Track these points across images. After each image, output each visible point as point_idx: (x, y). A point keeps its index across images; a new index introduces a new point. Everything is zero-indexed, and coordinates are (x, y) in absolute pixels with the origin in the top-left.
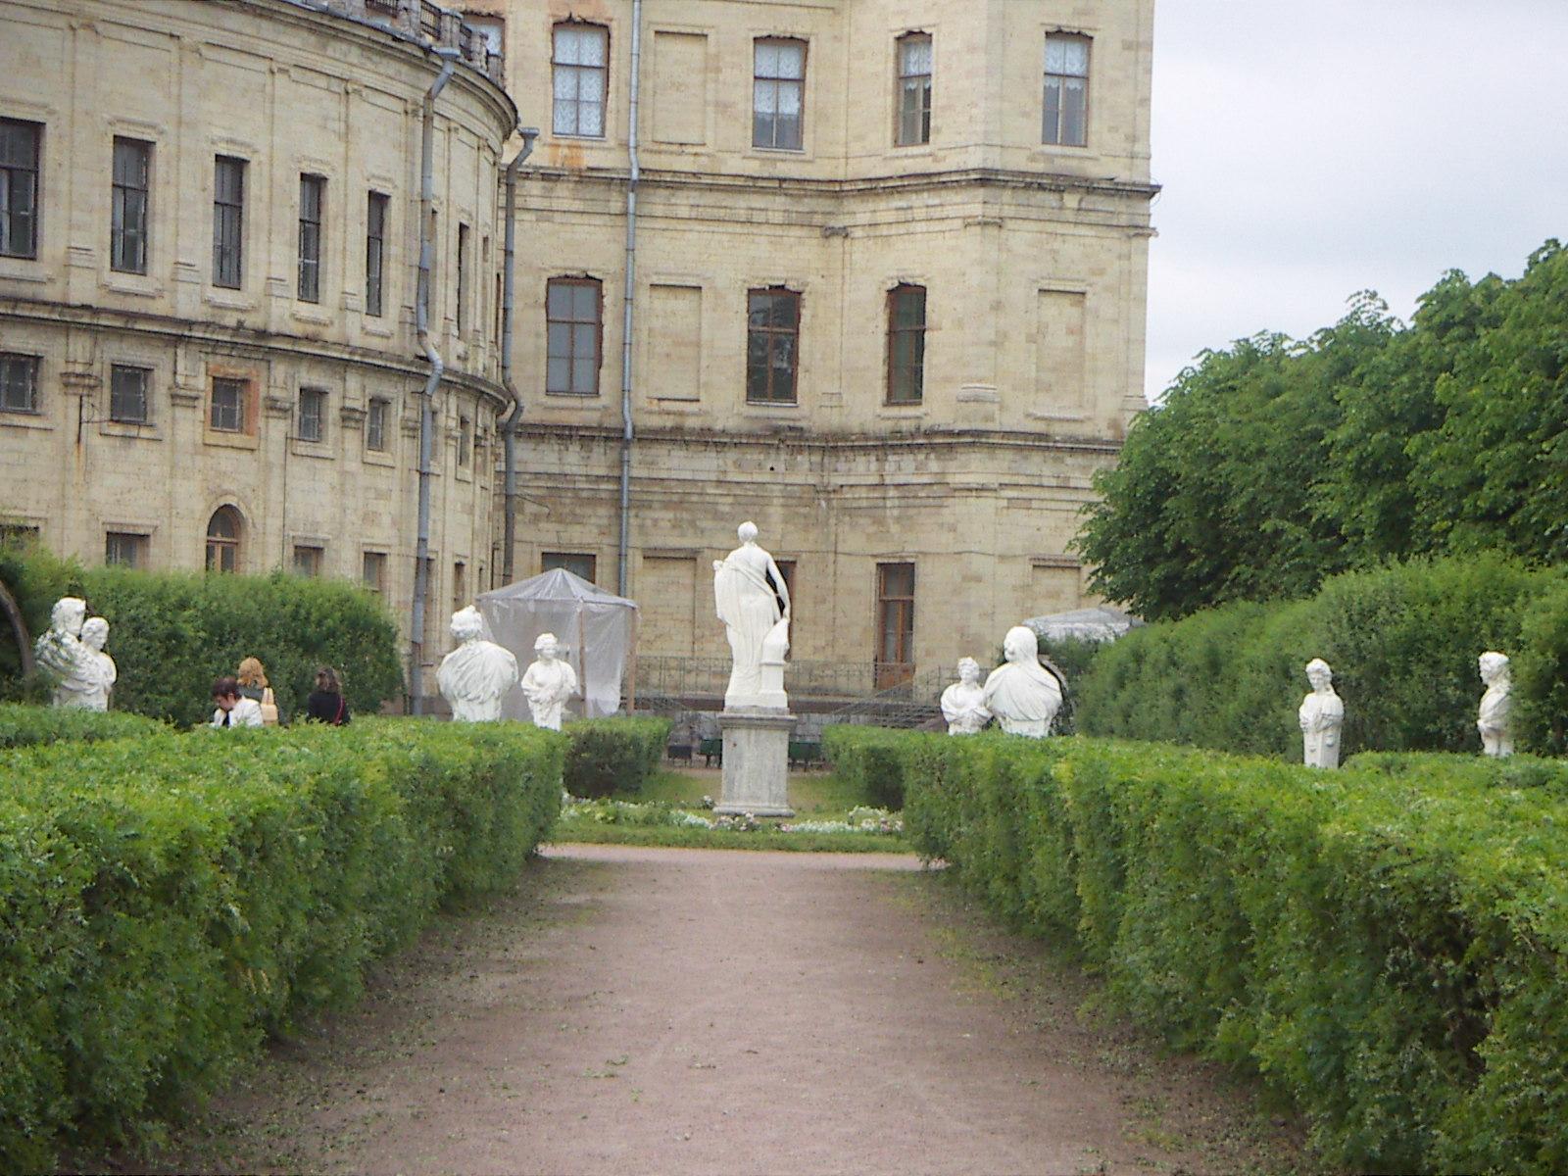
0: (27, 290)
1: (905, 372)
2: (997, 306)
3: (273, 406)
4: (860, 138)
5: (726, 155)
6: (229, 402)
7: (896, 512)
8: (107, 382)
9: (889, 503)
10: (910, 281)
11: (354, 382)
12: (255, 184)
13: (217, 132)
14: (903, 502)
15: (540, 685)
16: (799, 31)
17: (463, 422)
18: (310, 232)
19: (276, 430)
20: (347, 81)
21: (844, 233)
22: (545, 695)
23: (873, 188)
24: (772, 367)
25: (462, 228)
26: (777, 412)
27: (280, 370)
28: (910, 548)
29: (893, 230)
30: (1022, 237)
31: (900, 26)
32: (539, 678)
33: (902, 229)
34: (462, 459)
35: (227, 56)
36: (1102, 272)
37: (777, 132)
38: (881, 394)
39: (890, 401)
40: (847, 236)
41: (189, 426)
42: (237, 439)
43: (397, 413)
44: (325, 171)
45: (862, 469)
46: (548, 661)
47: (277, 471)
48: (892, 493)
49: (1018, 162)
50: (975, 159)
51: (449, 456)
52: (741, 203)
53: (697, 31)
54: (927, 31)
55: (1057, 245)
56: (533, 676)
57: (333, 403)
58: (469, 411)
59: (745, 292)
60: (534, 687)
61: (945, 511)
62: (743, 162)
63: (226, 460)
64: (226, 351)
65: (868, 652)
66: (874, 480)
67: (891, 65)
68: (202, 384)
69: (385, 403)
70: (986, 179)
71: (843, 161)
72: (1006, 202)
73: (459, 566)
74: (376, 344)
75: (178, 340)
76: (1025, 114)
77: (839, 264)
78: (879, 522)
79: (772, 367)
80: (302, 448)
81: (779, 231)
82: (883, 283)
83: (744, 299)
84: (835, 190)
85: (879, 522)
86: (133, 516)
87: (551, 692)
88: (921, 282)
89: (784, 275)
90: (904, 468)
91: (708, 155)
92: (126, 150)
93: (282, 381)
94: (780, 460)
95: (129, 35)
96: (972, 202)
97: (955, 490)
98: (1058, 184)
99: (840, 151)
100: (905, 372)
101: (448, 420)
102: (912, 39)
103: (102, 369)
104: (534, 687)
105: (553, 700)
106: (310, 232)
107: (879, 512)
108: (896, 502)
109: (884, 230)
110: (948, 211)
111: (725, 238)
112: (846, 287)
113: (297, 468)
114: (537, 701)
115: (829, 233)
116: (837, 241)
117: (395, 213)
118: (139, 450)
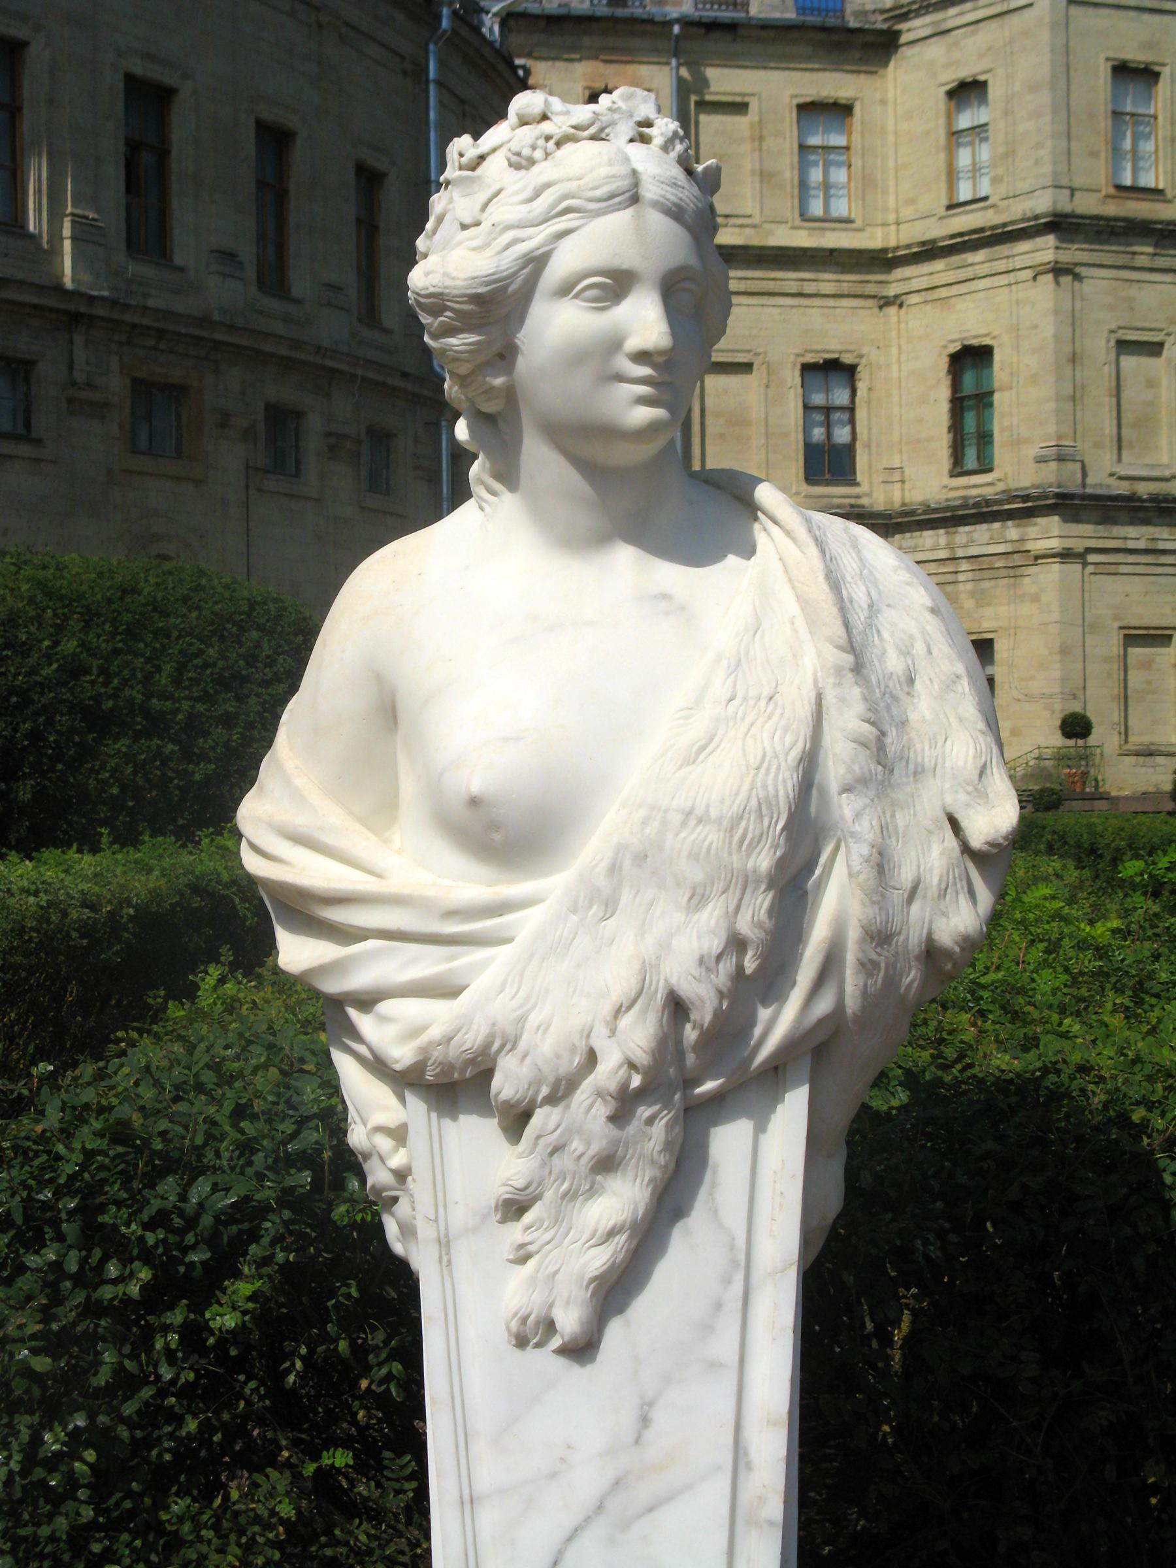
2: (1074, 359)
4: (912, 201)
5: (773, 226)
7: (969, 586)
9: (961, 577)
10: (975, 342)
14: (978, 575)
15: (503, 833)
18: (273, 193)
19: (229, 458)
20: (318, 9)
21: (896, 301)
22: (576, 973)
23: (929, 252)
28: (986, 625)
29: (954, 290)
30: (1098, 286)
32: (481, 733)
33: (964, 288)
39: (958, 468)
40: (901, 306)
44: (291, 121)
48: (964, 566)
49: (1087, 205)
50: (1042, 204)
52: (790, 279)
53: (738, 99)
54: (982, 78)
55: (1133, 291)
56: (388, 712)
57: (314, 423)
59: (799, 367)
60: (414, 866)
61: (1026, 580)
64: (151, 342)
66: (943, 554)
67: (942, 121)
68: (116, 384)
69: (389, 436)
70: (1060, 225)
71: (893, 227)
72: (1073, 253)
76: (1094, 154)
77: (894, 334)
81: (831, 302)
82: (945, 347)
83: (797, 373)
87: (684, 942)
88: (987, 341)
89: (839, 347)
91: (754, 226)
96: (1045, 249)
97: (1037, 558)
99: (892, 217)
102: (968, 91)
104: (414, 866)
105: (693, 1075)
106: (273, 193)
107: (949, 588)
108: (970, 575)
109: (943, 293)
110: (1018, 262)
111: (776, 311)
112: (903, 357)
114: (453, 1084)
115: (886, 302)
116: (892, 310)
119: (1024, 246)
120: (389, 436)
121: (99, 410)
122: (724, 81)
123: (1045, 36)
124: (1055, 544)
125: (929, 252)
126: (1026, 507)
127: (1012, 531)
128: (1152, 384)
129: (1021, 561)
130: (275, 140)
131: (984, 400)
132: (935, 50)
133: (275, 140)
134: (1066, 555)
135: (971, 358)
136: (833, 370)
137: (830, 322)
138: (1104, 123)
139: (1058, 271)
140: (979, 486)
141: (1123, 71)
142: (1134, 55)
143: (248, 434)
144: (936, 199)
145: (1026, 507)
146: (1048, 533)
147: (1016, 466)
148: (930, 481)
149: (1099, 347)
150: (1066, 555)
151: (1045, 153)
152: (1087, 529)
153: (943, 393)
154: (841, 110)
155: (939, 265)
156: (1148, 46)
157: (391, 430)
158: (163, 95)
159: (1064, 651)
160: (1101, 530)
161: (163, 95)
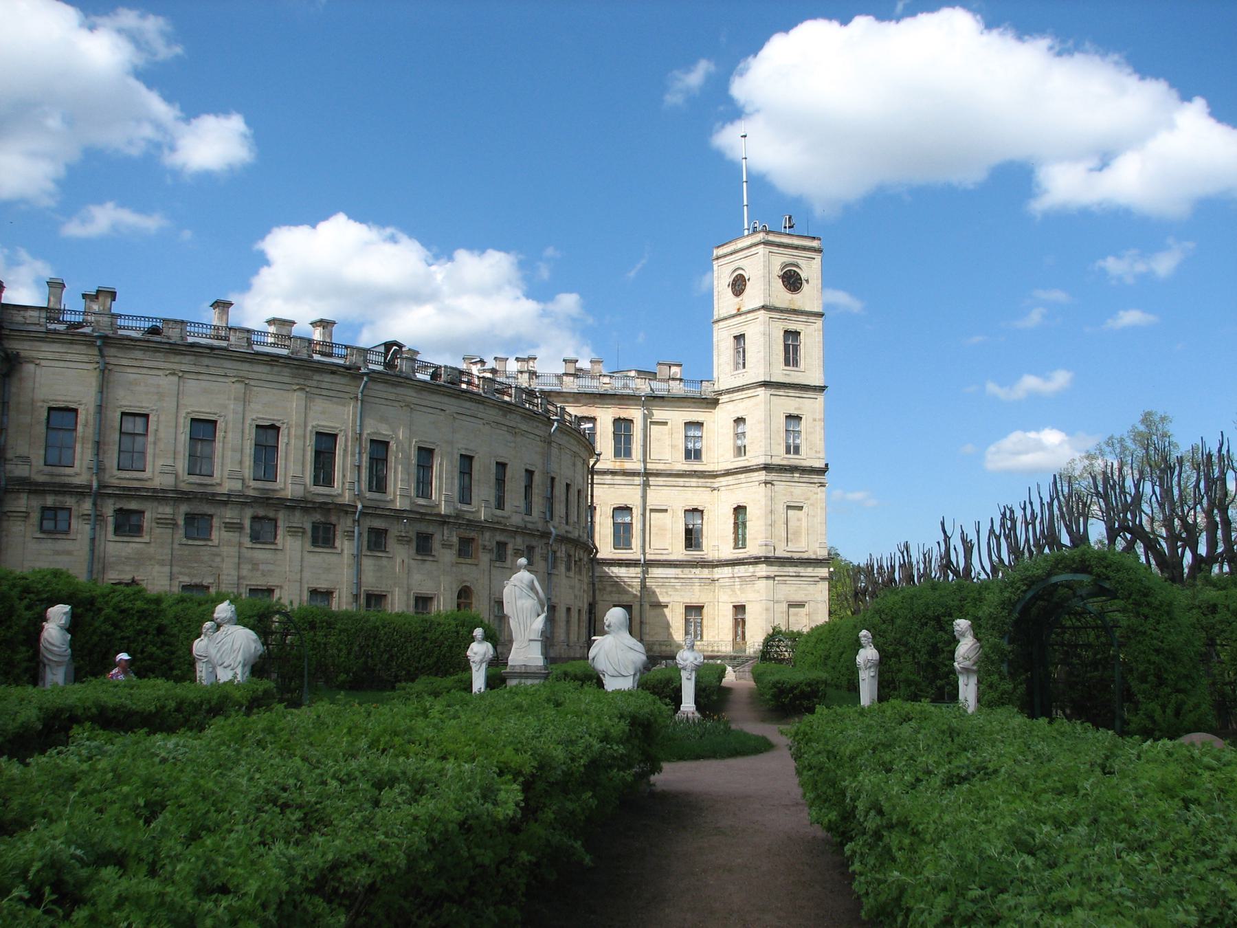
0: (382, 505)
1: (739, 539)
3: (484, 548)
6: (465, 548)
8: (414, 538)
11: (519, 540)
12: (476, 465)
13: (460, 446)
16: (700, 420)
17: (569, 556)
19: (485, 558)
22: (477, 658)
23: (728, 473)
24: (692, 538)
25: (568, 486)
26: (694, 554)
27: (487, 535)
30: (780, 487)
31: (735, 416)
32: (475, 650)
34: (568, 569)
35: (464, 417)
36: (808, 499)
37: (693, 454)
38: (732, 545)
41: (448, 556)
42: (469, 561)
43: (538, 551)
44: (506, 461)
45: (727, 571)
46: (480, 642)
47: (487, 573)
49: (776, 461)
50: (761, 460)
51: (562, 568)
52: (681, 481)
57: (510, 546)
58: (572, 553)
62: (682, 465)
63: (464, 569)
65: (730, 637)
68: (455, 540)
69: (533, 548)
70: (767, 468)
72: (772, 476)
73: (569, 610)
74: (529, 526)
75: (444, 523)
78: (733, 591)
79: (692, 538)
80: (497, 564)
84: (714, 475)
85: (733, 591)
86: (426, 589)
90: (741, 570)
92: (423, 452)
93: (487, 539)
94: (697, 571)
95: (424, 409)
96: (762, 476)
98: (792, 469)
100: (739, 539)
101: (562, 553)
102: (739, 421)
103: (412, 535)
105: (481, 662)
106: (500, 482)
113: (494, 571)
117: (537, 478)
118: (428, 565)
119: (756, 474)
120: (533, 548)
121: (450, 546)
122: (659, 414)
123: (763, 405)
124: (764, 574)
125: (728, 473)
126: (756, 561)
127: (751, 568)
128: (799, 520)
129: (754, 578)
130: (502, 466)
131: (744, 524)
132: (730, 406)
133: (502, 466)
134: (768, 578)
135: (739, 510)
136: (696, 511)
137: (695, 495)
138: (783, 434)
139: (766, 483)
140: (740, 553)
141: (790, 417)
142: (795, 413)
143: (491, 551)
144: (730, 453)
145: (756, 561)
146: (762, 570)
147: (754, 548)
148: (728, 552)
149: (781, 508)
150: (768, 578)
151: (762, 444)
152: (775, 568)
153: (732, 521)
154: (699, 425)
155: (730, 478)
156: (799, 409)
157: (473, 640)
158: (470, 458)
159: (767, 609)
160: (780, 569)
161: (470, 458)
